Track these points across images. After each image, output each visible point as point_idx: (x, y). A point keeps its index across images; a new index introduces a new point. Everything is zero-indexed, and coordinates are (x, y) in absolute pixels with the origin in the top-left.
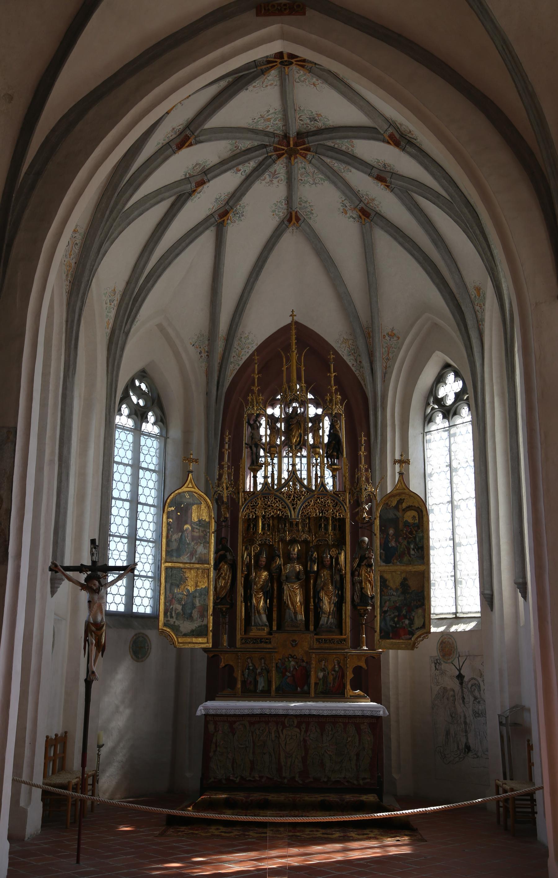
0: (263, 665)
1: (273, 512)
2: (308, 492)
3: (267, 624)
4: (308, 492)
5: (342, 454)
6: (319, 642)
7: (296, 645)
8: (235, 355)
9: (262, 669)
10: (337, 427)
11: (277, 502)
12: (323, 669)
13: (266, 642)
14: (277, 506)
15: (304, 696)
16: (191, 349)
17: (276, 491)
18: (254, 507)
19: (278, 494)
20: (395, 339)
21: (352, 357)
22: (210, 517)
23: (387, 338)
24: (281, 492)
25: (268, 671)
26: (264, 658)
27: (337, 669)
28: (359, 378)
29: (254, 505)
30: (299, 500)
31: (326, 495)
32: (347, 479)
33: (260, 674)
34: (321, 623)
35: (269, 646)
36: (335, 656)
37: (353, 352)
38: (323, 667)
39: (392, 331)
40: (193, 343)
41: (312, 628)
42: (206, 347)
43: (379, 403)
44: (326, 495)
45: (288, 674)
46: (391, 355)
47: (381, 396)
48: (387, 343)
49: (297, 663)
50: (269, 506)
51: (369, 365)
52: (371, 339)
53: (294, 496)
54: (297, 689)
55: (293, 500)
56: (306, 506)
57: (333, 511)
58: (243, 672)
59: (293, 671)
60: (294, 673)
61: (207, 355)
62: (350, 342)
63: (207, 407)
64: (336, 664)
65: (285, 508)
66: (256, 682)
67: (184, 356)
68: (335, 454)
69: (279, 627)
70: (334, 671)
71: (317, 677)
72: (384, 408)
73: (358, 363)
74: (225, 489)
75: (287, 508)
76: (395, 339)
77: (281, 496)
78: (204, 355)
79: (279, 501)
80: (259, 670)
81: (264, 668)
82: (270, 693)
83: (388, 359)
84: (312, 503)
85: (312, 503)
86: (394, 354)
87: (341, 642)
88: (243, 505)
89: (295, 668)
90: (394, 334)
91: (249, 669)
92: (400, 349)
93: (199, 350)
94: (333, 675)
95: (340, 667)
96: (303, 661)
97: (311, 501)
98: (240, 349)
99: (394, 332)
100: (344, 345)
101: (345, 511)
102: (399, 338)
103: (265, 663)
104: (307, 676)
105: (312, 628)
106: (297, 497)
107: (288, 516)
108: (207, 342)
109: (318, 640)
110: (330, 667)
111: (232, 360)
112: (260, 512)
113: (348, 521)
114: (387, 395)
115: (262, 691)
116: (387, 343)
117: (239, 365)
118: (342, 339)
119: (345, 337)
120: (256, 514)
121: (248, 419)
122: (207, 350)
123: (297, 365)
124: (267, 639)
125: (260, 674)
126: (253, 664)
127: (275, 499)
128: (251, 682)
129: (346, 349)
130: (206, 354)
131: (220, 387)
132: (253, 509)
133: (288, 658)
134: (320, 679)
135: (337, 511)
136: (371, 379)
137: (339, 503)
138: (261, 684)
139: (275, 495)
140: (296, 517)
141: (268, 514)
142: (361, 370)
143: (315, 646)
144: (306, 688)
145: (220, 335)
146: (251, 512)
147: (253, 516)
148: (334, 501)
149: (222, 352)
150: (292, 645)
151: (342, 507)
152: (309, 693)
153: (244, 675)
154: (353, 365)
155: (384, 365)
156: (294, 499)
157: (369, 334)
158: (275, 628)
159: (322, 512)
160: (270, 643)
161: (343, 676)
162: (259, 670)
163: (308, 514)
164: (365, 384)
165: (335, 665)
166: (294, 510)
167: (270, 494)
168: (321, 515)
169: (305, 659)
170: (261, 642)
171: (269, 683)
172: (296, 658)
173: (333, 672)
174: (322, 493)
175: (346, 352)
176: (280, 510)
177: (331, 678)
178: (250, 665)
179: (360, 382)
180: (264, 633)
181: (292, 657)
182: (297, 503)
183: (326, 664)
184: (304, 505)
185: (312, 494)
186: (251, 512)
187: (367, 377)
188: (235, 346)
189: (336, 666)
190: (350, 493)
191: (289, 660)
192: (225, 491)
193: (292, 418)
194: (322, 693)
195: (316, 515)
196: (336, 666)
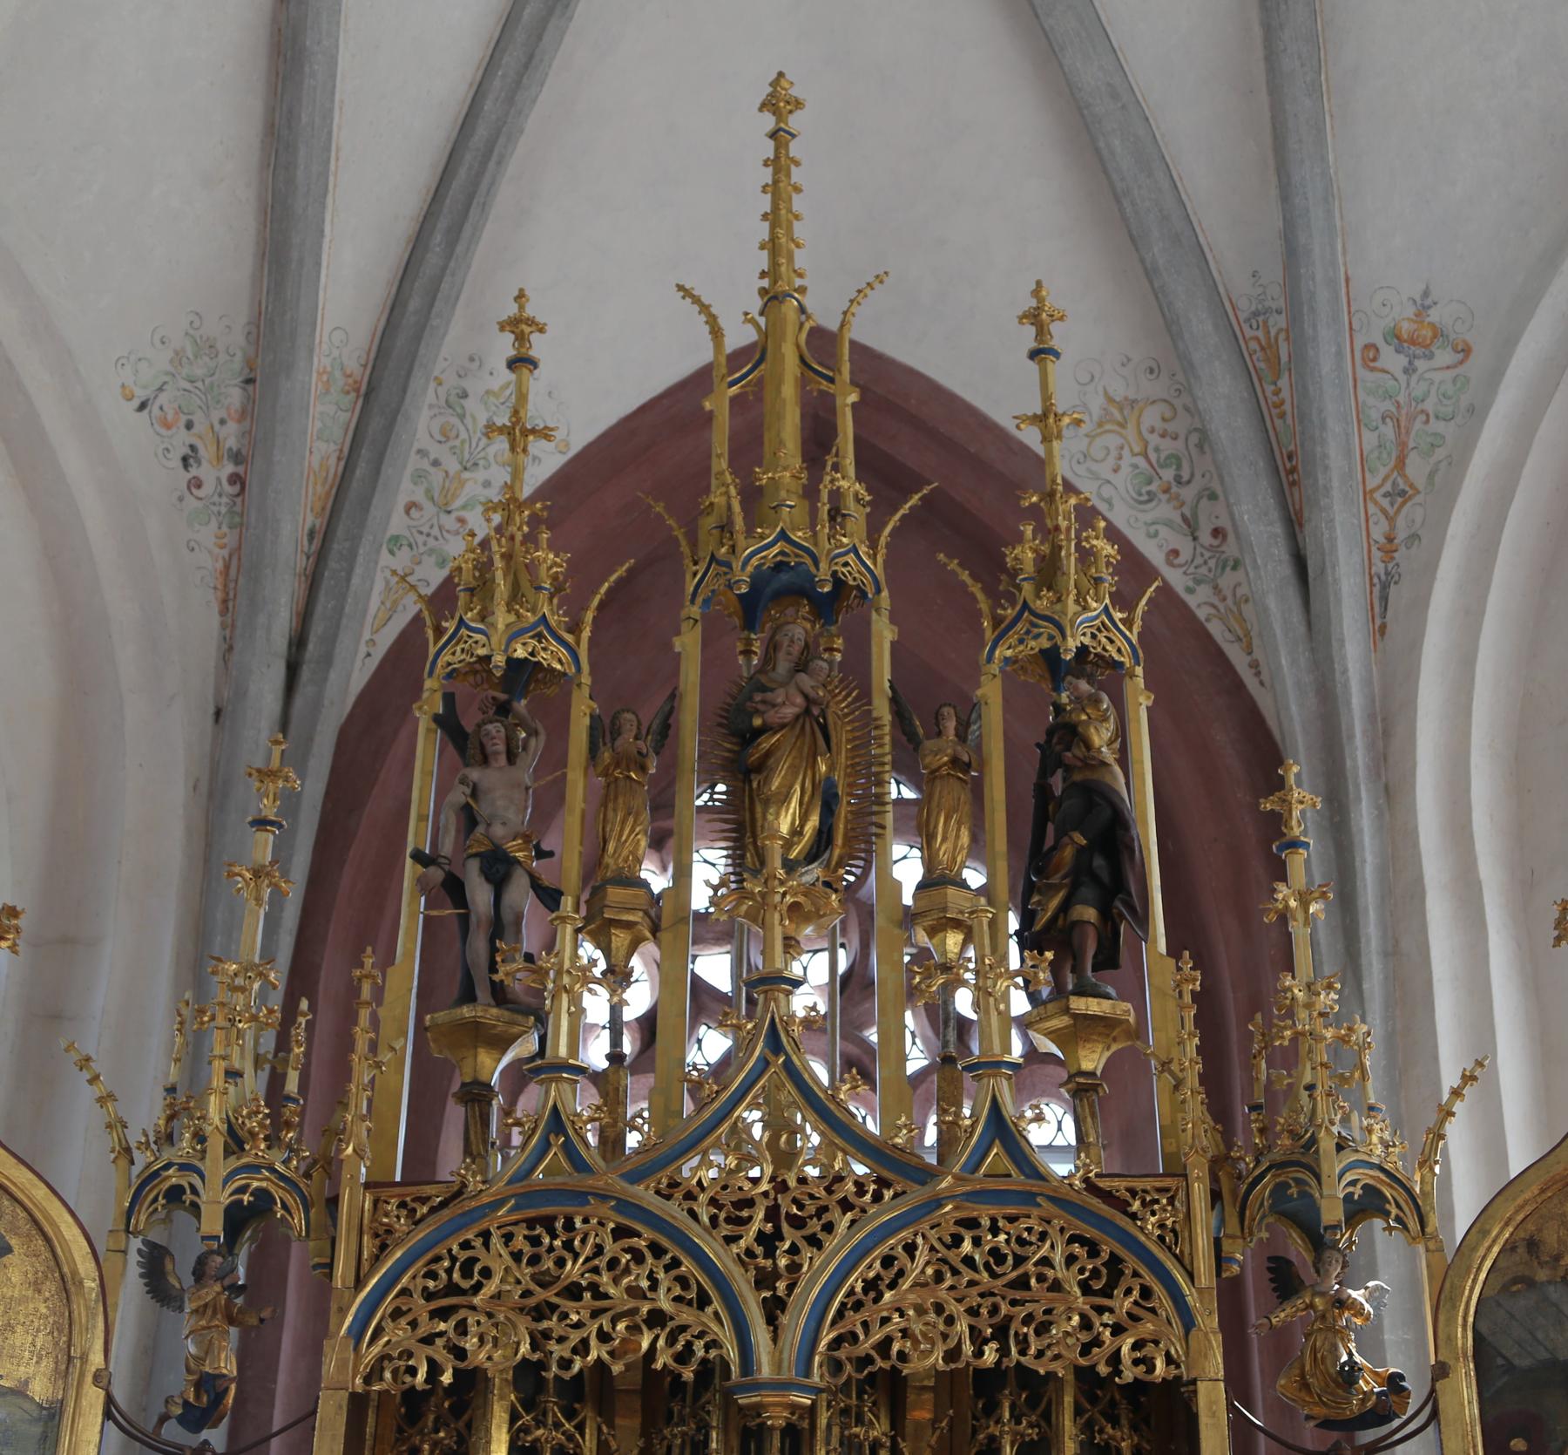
1: (604, 1337)
2: (883, 1183)
4: (883, 1183)
5: (1143, 919)
8: (419, 496)
10: (1101, 737)
11: (638, 1258)
14: (633, 1291)
16: (132, 435)
17: (635, 1177)
18: (449, 1300)
19: (644, 1194)
20: (1444, 356)
21: (1164, 510)
22: (67, 1363)
23: (1392, 360)
24: (674, 1185)
28: (1215, 629)
29: (452, 1289)
30: (815, 1242)
31: (1029, 1198)
32: (1192, 1080)
37: (1168, 474)
39: (1422, 310)
40: (141, 394)
42: (232, 427)
43: (1358, 756)
44: (1029, 1198)
46: (1416, 469)
47: (1371, 717)
48: (1388, 396)
50: (574, 1292)
51: (1279, 529)
52: (1283, 382)
53: (772, 1214)
55: (768, 1242)
56: (871, 1285)
57: (1086, 1324)
61: (234, 479)
62: (1151, 417)
63: (214, 792)
65: (703, 1301)
67: (73, 460)
68: (1090, 914)
72: (1394, 792)
73: (1206, 537)
74: (216, 1144)
75: (717, 1305)
76: (1444, 356)
77: (674, 1210)
78: (214, 474)
79: (657, 1251)
83: (1401, 495)
84: (920, 1266)
85: (920, 1266)
86: (1440, 453)
88: (359, 1283)
90: (1438, 333)
92: (1476, 414)
93: (180, 440)
97: (910, 1249)
98: (453, 466)
99: (1434, 316)
100: (1112, 441)
101: (1188, 1323)
102: (1466, 351)
106: (797, 1223)
107: (725, 1365)
108: (235, 396)
111: (398, 523)
112: (496, 1352)
113: (1212, 1401)
114: (1411, 704)
116: (1388, 396)
117: (442, 563)
118: (1096, 404)
119: (1119, 391)
120: (460, 1354)
121: (449, 699)
122: (231, 443)
123: (803, 382)
127: (620, 1233)
129: (1127, 459)
130: (230, 468)
131: (306, 673)
132: (442, 1314)
135: (1118, 1330)
136: (1297, 617)
137: (1131, 1262)
139: (624, 1206)
140: (784, 1377)
141: (558, 1351)
142: (1227, 580)
145: (320, 361)
146: (428, 1340)
147: (434, 1369)
148: (1093, 1250)
149: (334, 467)
151: (1158, 1289)
154: (1175, 553)
155: (1378, 533)
156: (778, 1235)
157: (1269, 348)
159: (1001, 1333)
163: (884, 1346)
164: (1255, 665)
166: (771, 1320)
167: (581, 1197)
168: (990, 1355)
174: (992, 1185)
175: (1123, 480)
176: (657, 1319)
179: (1220, 655)
182: (794, 1268)
184: (855, 1281)
185: (918, 1195)
186: (428, 1340)
187: (1272, 603)
188: (422, 439)
190: (1216, 1197)
192: (217, 1164)
193: (764, 689)
195: (952, 1355)
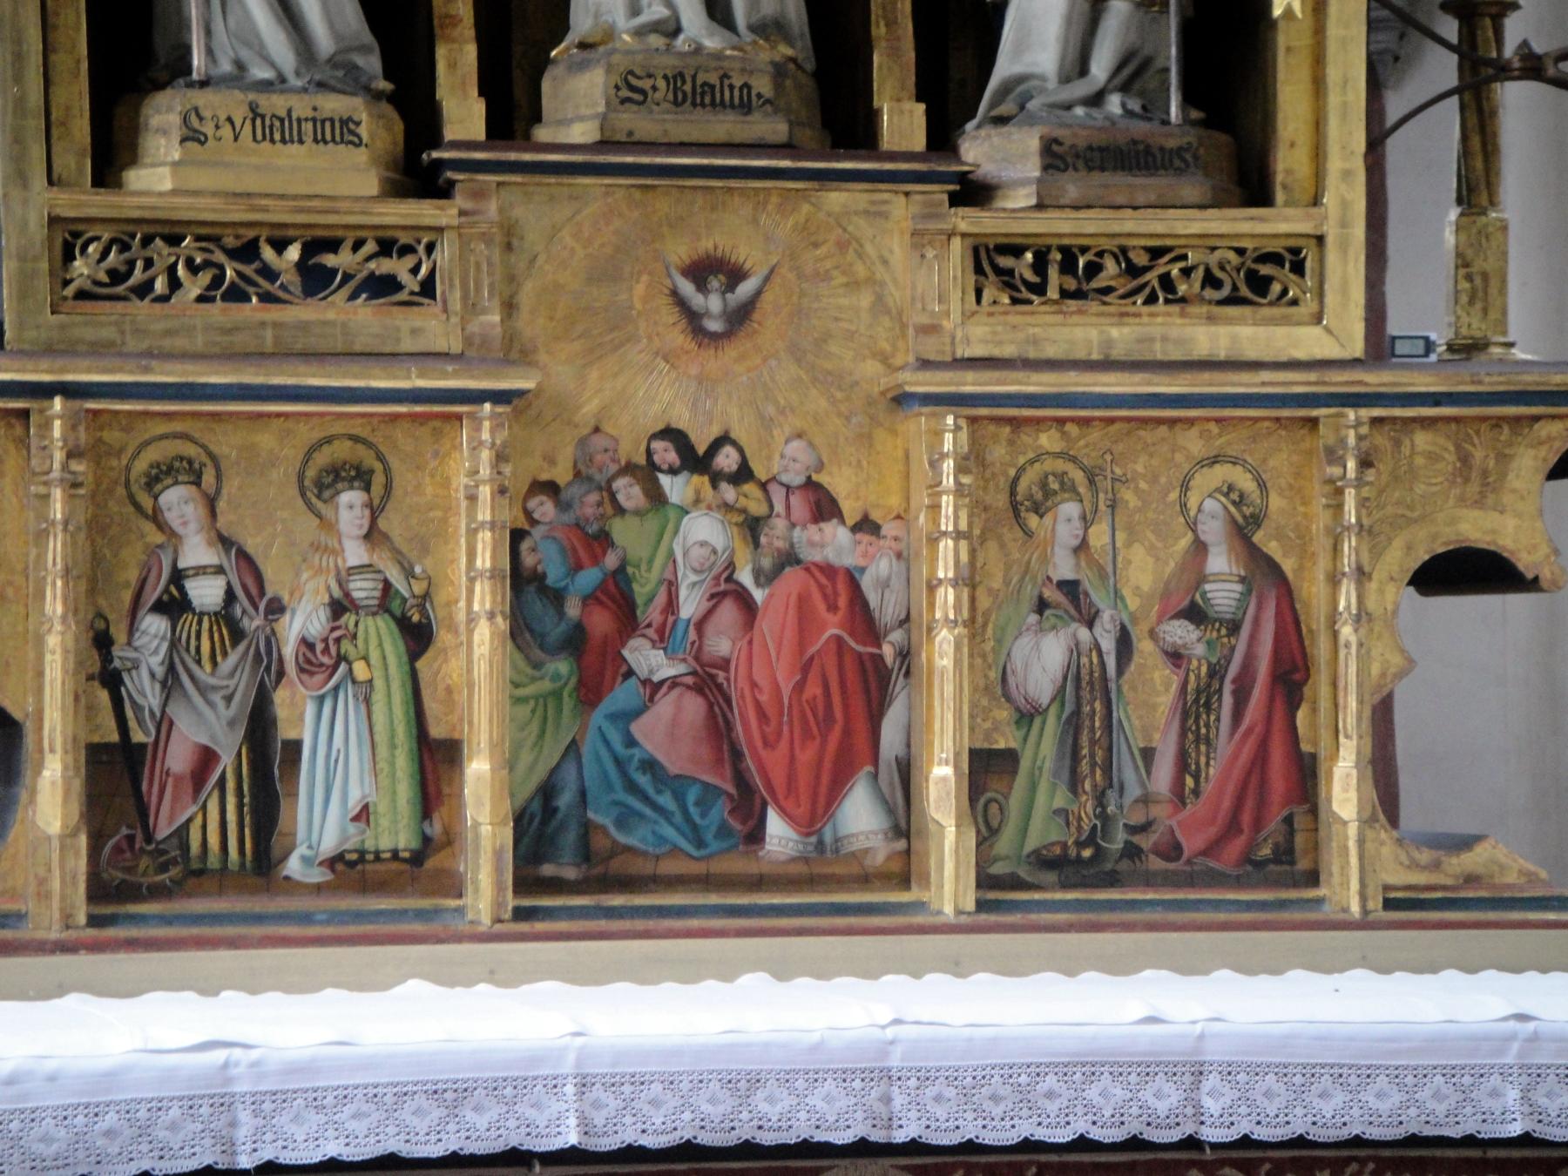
0: (355, 553)
3: (372, 63)
6: (1005, 275)
7: (740, 316)
9: (339, 608)
12: (1070, 588)
13: (382, 287)
15: (853, 900)
25: (417, 636)
26: (362, 478)
27: (1223, 595)
33: (325, 660)
34: (1004, 67)
35: (431, 327)
36: (1193, 443)
38: (1064, 568)
41: (902, 122)
45: (646, 658)
49: (753, 527)
54: (756, 836)
58: (103, 642)
59: (701, 624)
60: (720, 644)
64: (1213, 529)
66: (269, 764)
69: (512, 110)
70: (1195, 614)
71: (995, 683)
80: (304, 620)
81: (363, 589)
82: (453, 885)
87: (1260, 285)
89: (727, 591)
91: (175, 605)
94: (1176, 657)
95: (1263, 572)
96: (824, 507)
103: (373, 536)
104: (864, 673)
105: (902, 122)
109: (992, 262)
110: (1143, 573)
115: (350, 869)
124: (386, 247)
125: (325, 660)
126: (225, 542)
128: (207, 758)
133: (646, 474)
134: (1027, 716)
138: (342, 788)
143: (979, 337)
144: (860, 816)
150: (693, 318)
152: (905, 870)
153: (112, 680)
158: (464, 115)
160: (427, 288)
161: (1292, 675)
162: (304, 620)
165: (1200, 548)
169: (839, 482)
170: (315, 280)
171: (436, 760)
172: (743, 474)
173: (1181, 632)
177: (1150, 703)
178: (197, 551)
180: (344, 179)
181: (695, 461)
183: (1099, 536)
189: (1219, 561)
191: (657, 497)
194: (1058, 865)
196: (1219, 561)
